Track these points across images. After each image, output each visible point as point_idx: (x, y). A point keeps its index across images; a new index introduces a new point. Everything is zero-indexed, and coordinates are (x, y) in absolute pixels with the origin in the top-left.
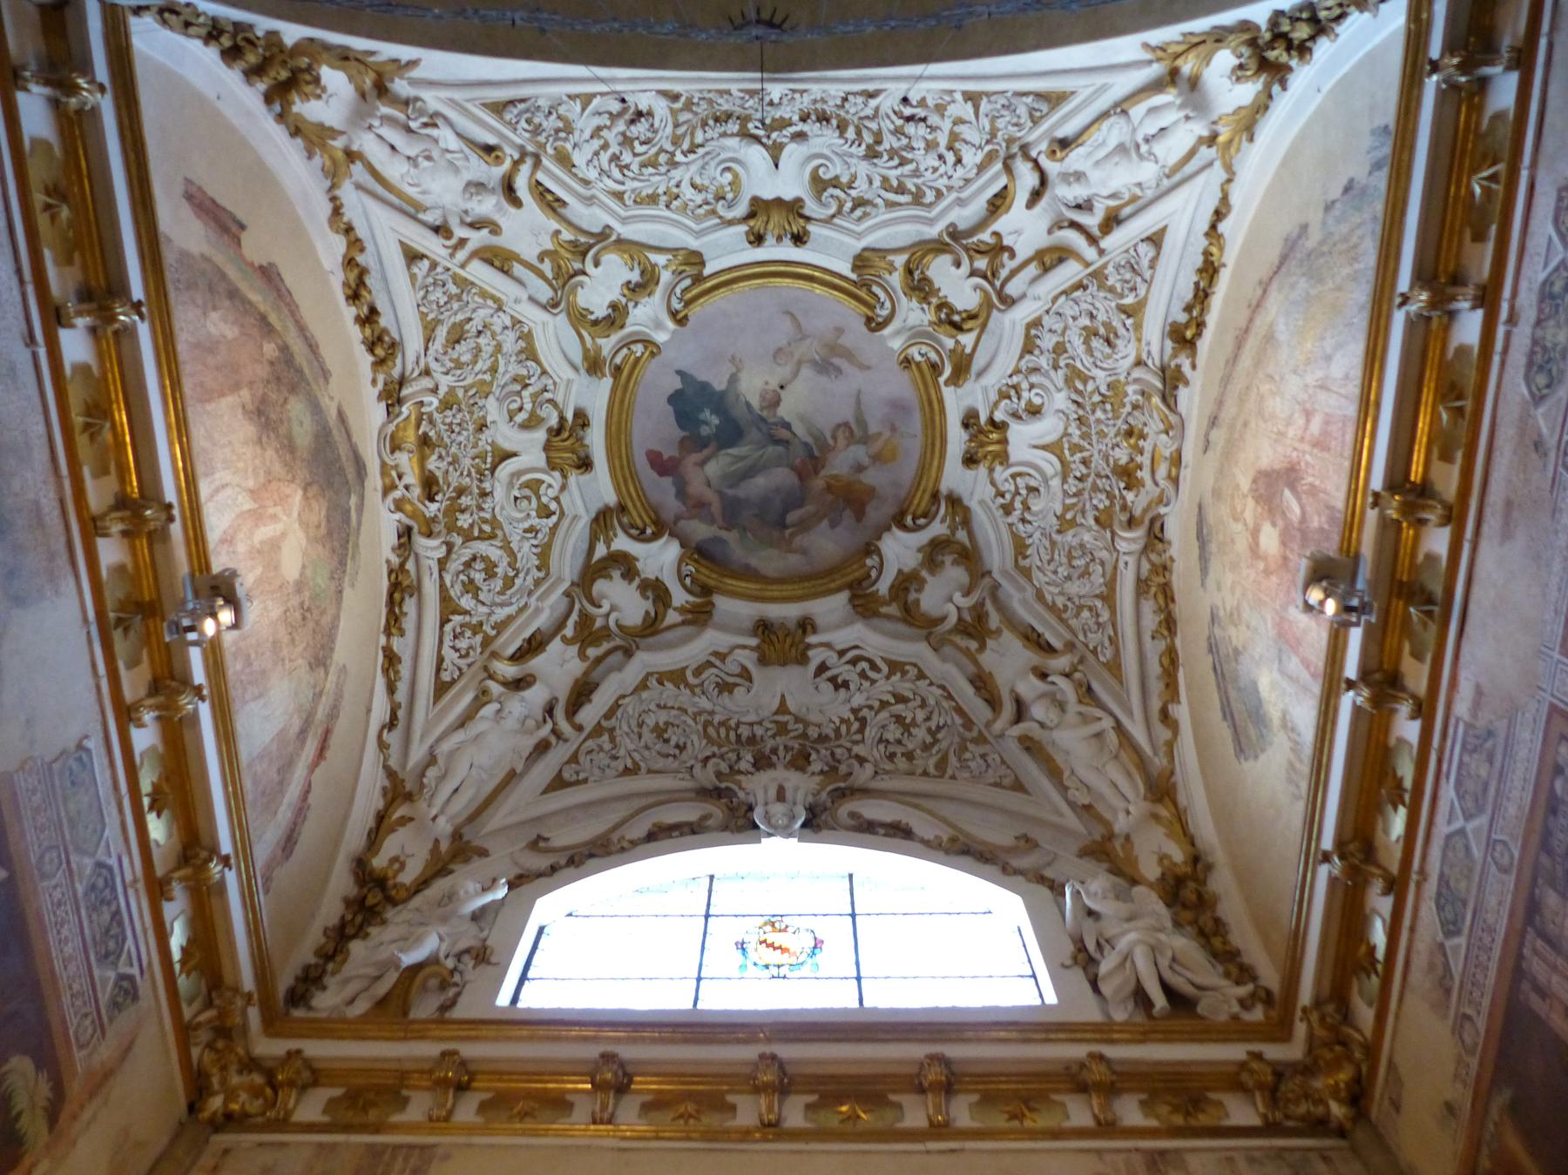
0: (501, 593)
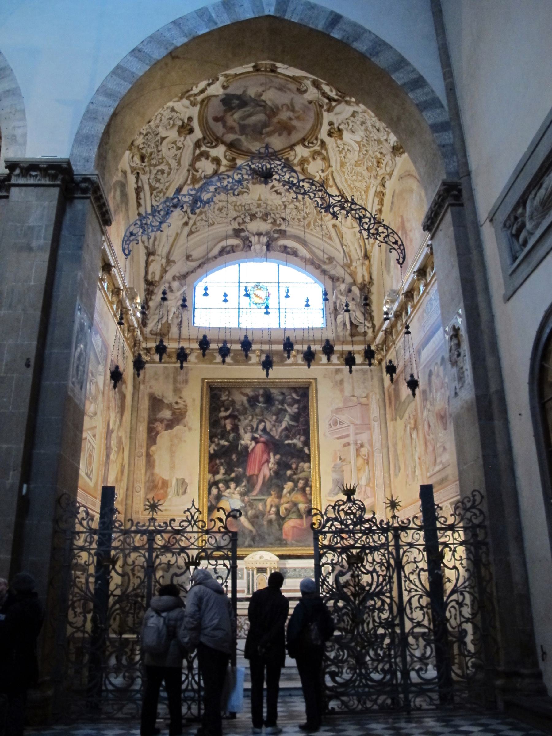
0: (167, 177)
